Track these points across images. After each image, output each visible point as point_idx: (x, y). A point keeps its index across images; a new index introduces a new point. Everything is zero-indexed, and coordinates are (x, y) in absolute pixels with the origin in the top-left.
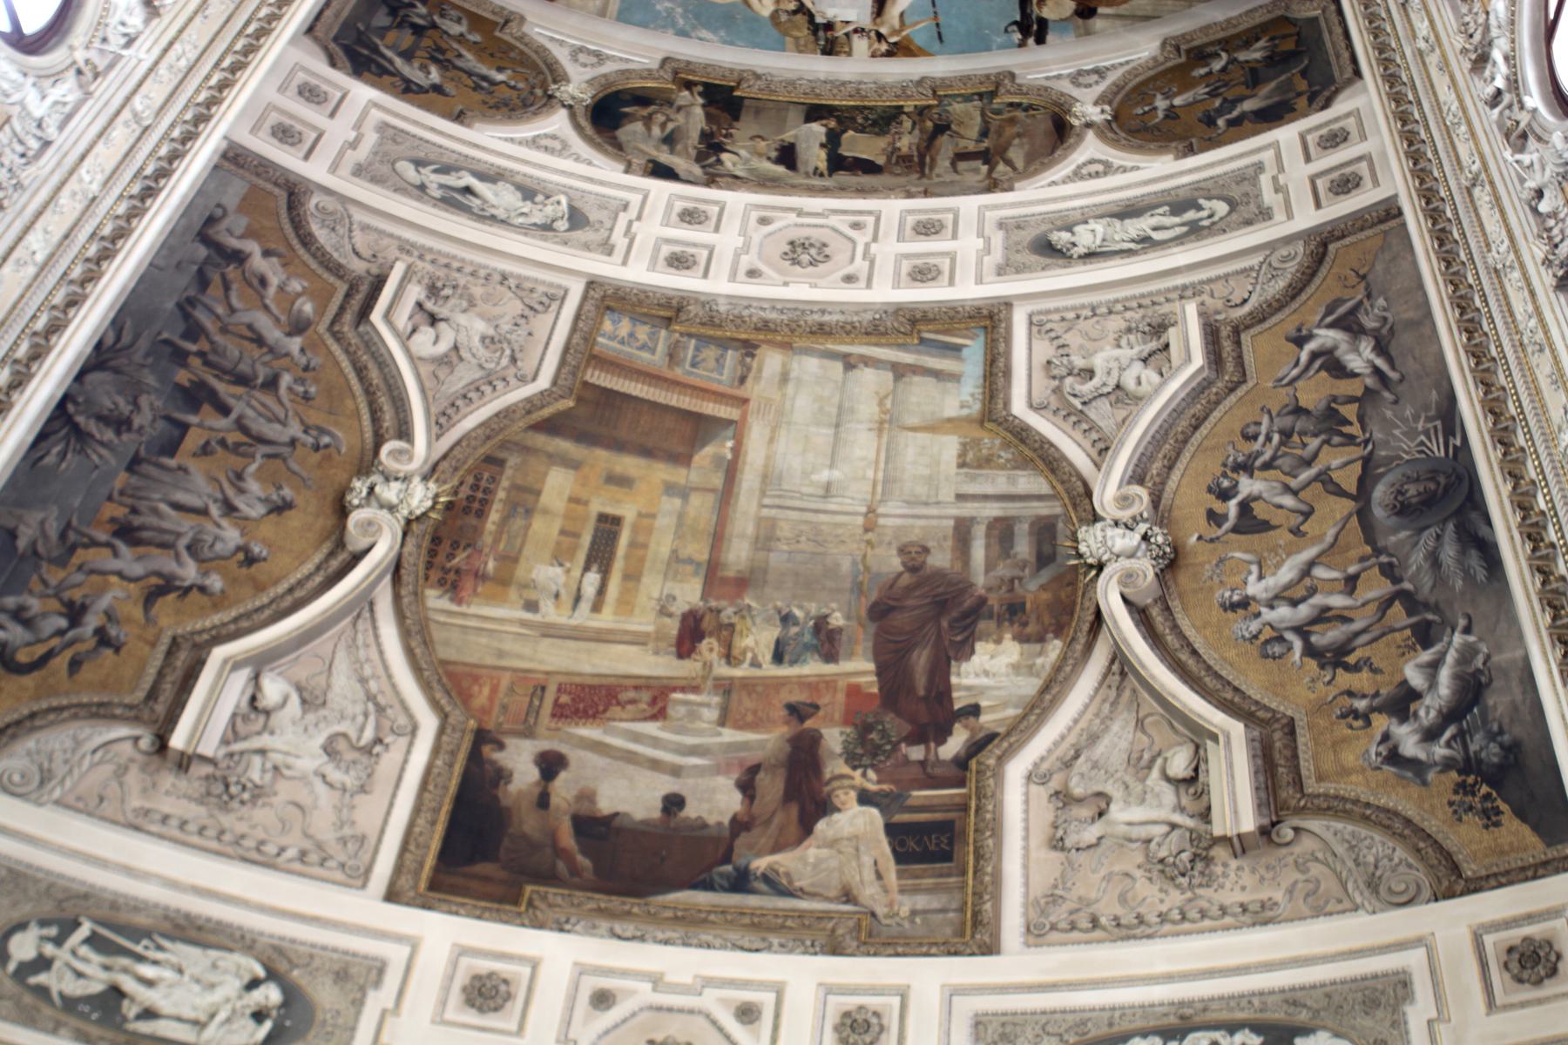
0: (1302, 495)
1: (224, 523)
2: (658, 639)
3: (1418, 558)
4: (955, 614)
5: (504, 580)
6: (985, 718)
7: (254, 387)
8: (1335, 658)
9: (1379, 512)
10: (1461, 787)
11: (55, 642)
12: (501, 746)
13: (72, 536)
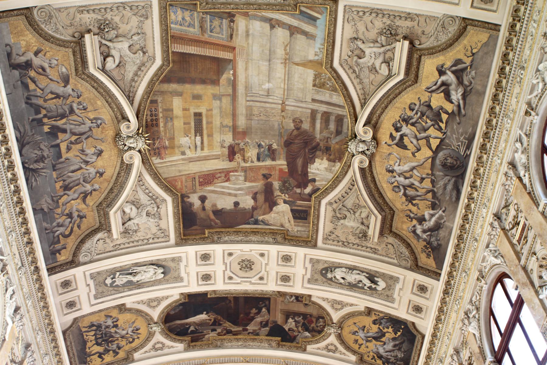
0: (419, 141)
1: (88, 168)
2: (223, 156)
3: (441, 183)
4: (310, 147)
5: (173, 147)
6: (317, 183)
7: (67, 117)
8: (410, 199)
9: (438, 162)
10: (425, 246)
11: (71, 225)
12: (189, 197)
13: (55, 199)
